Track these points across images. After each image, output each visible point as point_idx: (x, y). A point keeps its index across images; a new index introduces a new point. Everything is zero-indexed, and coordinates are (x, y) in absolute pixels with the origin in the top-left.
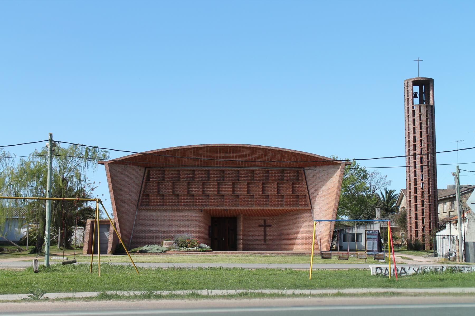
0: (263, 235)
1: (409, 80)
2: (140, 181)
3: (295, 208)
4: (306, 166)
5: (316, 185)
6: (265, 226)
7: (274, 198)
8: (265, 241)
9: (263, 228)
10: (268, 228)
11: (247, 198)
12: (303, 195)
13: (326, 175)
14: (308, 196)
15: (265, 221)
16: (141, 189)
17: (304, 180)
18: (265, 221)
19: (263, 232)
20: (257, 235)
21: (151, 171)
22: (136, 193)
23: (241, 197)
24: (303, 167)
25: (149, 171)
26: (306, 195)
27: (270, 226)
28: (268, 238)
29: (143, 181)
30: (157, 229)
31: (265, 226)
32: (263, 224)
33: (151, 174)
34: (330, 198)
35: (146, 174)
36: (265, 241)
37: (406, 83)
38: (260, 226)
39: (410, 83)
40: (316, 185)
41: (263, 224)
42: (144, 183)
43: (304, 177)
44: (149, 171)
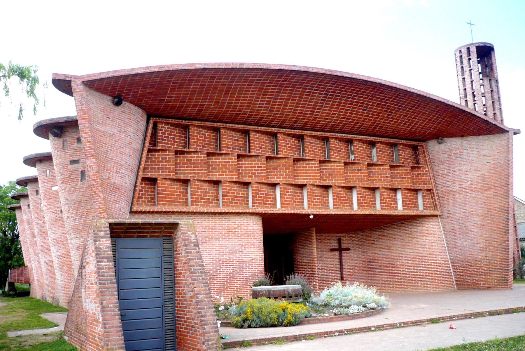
0: (338, 266)
1: (470, 45)
2: (137, 145)
3: (415, 213)
4: (430, 139)
5: (455, 171)
6: (340, 250)
9: (337, 253)
13: (475, 152)
15: (339, 241)
16: (140, 164)
18: (339, 241)
19: (337, 262)
20: (329, 266)
21: (160, 126)
24: (425, 139)
25: (155, 125)
27: (348, 249)
28: (345, 272)
29: (144, 147)
31: (340, 250)
32: (337, 246)
33: (160, 133)
34: (491, 192)
35: (150, 132)
37: (464, 50)
38: (332, 250)
39: (473, 50)
40: (455, 171)
41: (337, 246)
42: (145, 152)
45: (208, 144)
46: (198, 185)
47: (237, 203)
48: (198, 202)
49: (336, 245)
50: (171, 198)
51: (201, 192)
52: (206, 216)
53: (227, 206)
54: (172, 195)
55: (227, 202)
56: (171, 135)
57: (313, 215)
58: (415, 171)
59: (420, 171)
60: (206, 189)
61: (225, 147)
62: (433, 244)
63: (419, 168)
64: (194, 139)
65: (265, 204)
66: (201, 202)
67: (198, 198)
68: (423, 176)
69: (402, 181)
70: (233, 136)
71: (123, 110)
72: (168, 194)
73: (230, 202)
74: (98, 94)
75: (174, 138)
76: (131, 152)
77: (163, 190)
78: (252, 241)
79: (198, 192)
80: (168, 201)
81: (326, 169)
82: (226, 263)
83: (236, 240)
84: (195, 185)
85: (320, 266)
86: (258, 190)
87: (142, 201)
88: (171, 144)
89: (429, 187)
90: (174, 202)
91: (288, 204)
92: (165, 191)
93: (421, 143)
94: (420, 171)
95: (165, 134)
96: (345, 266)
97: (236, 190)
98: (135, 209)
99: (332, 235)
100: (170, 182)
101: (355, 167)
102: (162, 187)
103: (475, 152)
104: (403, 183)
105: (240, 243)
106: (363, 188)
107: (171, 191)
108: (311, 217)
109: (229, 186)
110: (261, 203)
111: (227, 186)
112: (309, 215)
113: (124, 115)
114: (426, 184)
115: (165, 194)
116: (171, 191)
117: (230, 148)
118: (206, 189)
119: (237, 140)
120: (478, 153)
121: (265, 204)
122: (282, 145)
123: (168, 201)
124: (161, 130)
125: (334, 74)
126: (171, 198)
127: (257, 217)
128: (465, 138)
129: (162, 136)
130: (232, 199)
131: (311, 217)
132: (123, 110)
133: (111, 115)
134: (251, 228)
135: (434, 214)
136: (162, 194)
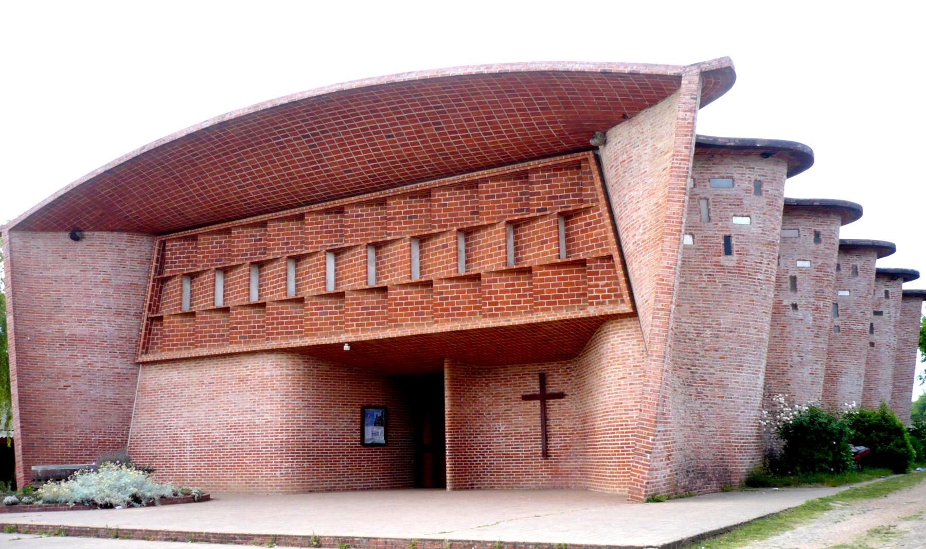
6: (544, 397)
7: (499, 285)
8: (546, 454)
9: (538, 403)
10: (553, 404)
11: (415, 295)
12: (602, 259)
14: (617, 259)
17: (601, 197)
19: (537, 420)
20: (521, 430)
21: (169, 244)
22: (118, 314)
23: (392, 293)
25: (163, 244)
26: (610, 257)
27: (561, 395)
28: (555, 442)
30: (181, 424)
31: (544, 397)
33: (168, 254)
36: (546, 454)
38: (526, 398)
41: (537, 389)
43: (598, 184)
44: (163, 244)
45: (225, 255)
46: (206, 318)
47: (254, 337)
48: (206, 342)
49: (534, 387)
50: (181, 340)
51: (210, 327)
52: (215, 361)
53: (236, 343)
54: (182, 335)
55: (236, 338)
56: (183, 253)
57: (350, 344)
58: (582, 220)
59: (591, 218)
60: (219, 322)
61: (238, 255)
62: (622, 382)
63: (587, 210)
64: (203, 253)
65: (291, 333)
66: (210, 341)
67: (205, 337)
68: (595, 228)
69: (541, 248)
70: (251, 236)
71: (89, 243)
72: (177, 336)
73: (241, 338)
74: (49, 235)
75: (188, 257)
76: (111, 291)
77: (169, 331)
78: (267, 394)
79: (206, 327)
80: (176, 345)
81: (388, 256)
82: (235, 428)
83: (248, 393)
84: (202, 318)
85: (503, 428)
86: (277, 313)
87: (158, 348)
88: (183, 266)
89: (607, 250)
90: (185, 344)
91: (319, 329)
92: (173, 331)
93: (579, 156)
94: (591, 218)
95: (175, 254)
96: (554, 428)
97: (254, 317)
98: (140, 359)
99: (529, 368)
100: (179, 319)
101: (439, 242)
102: (169, 327)
103: (649, 150)
104: (544, 254)
105: (252, 397)
106: (450, 279)
107: (181, 331)
108: (346, 348)
109: (241, 313)
110: (282, 333)
111: (237, 314)
112: (343, 344)
113: (92, 248)
114: (601, 245)
115: (173, 336)
116: (181, 331)
117: (246, 255)
118: (219, 322)
119: (260, 240)
120: (655, 148)
121: (291, 333)
122: (312, 233)
123: (176, 345)
124: (170, 250)
125: (262, 108)
126: (181, 340)
127: (279, 356)
128: (635, 120)
129: (171, 258)
130: (245, 332)
131: (346, 348)
132: (89, 243)
133: (69, 255)
134: (267, 373)
135: (615, 312)
136: (169, 336)
